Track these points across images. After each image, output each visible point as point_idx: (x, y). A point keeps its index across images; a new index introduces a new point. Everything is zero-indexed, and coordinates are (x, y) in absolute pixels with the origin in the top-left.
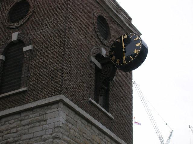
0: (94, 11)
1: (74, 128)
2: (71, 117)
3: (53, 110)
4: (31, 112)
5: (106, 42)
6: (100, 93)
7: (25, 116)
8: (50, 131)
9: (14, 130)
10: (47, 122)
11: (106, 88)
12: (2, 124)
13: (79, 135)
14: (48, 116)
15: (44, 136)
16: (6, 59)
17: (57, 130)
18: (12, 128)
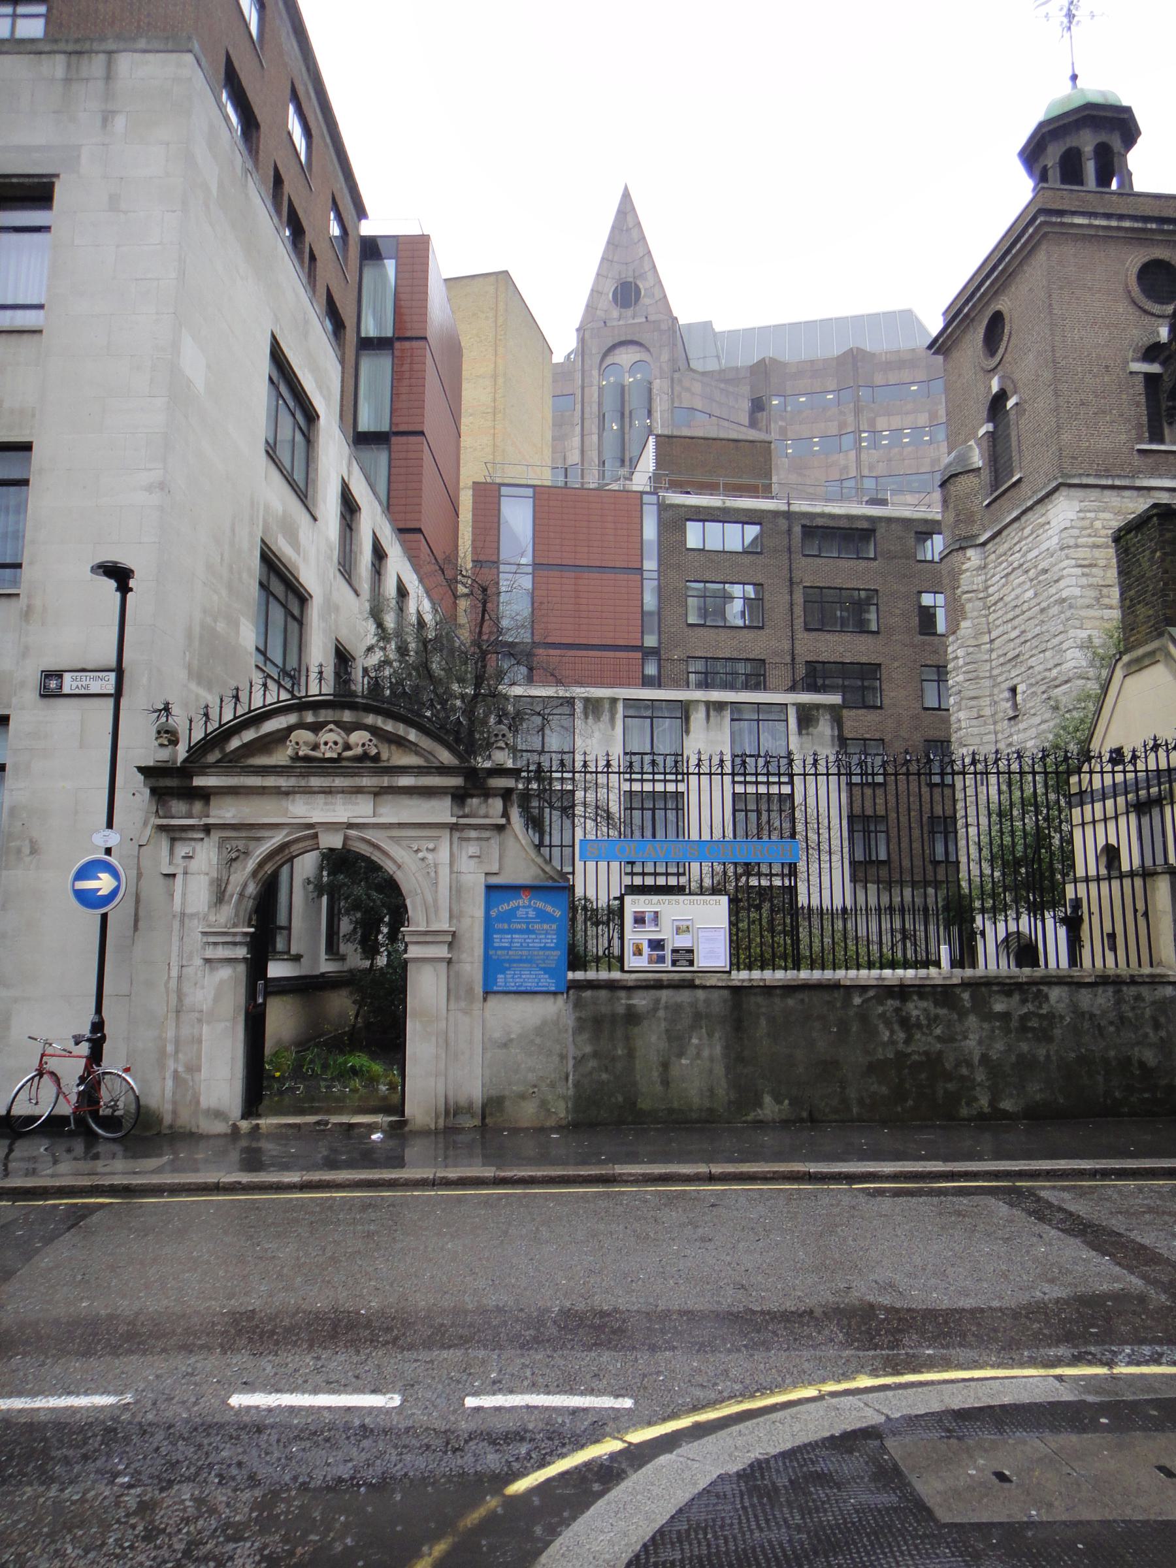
8: (1055, 540)
9: (1017, 548)
14: (1050, 515)
16: (995, 427)
17: (1064, 535)
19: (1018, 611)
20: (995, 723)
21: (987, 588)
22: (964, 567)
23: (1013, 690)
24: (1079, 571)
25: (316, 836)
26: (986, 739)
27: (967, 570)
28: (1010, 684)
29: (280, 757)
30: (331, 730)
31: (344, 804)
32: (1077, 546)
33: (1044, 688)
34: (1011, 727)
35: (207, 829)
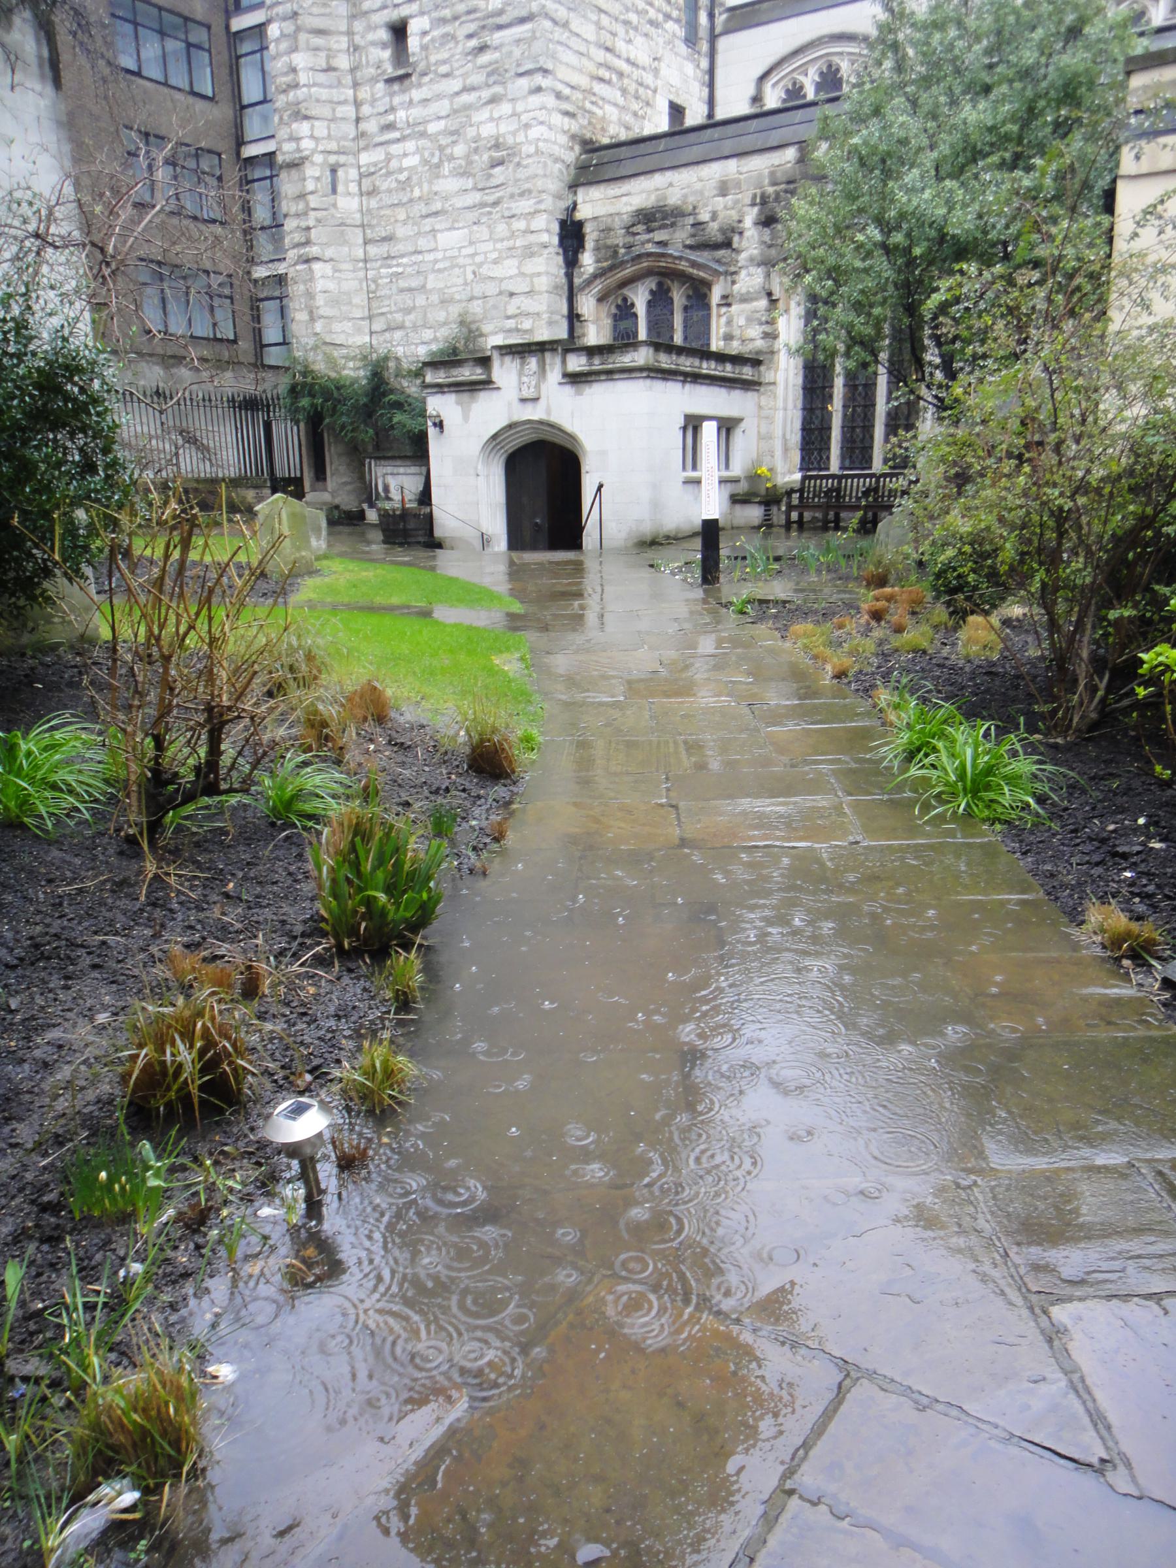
20: (356, 85)
23: (399, 31)
26: (342, 111)
28: (395, 15)
33: (471, 27)
34: (392, 95)
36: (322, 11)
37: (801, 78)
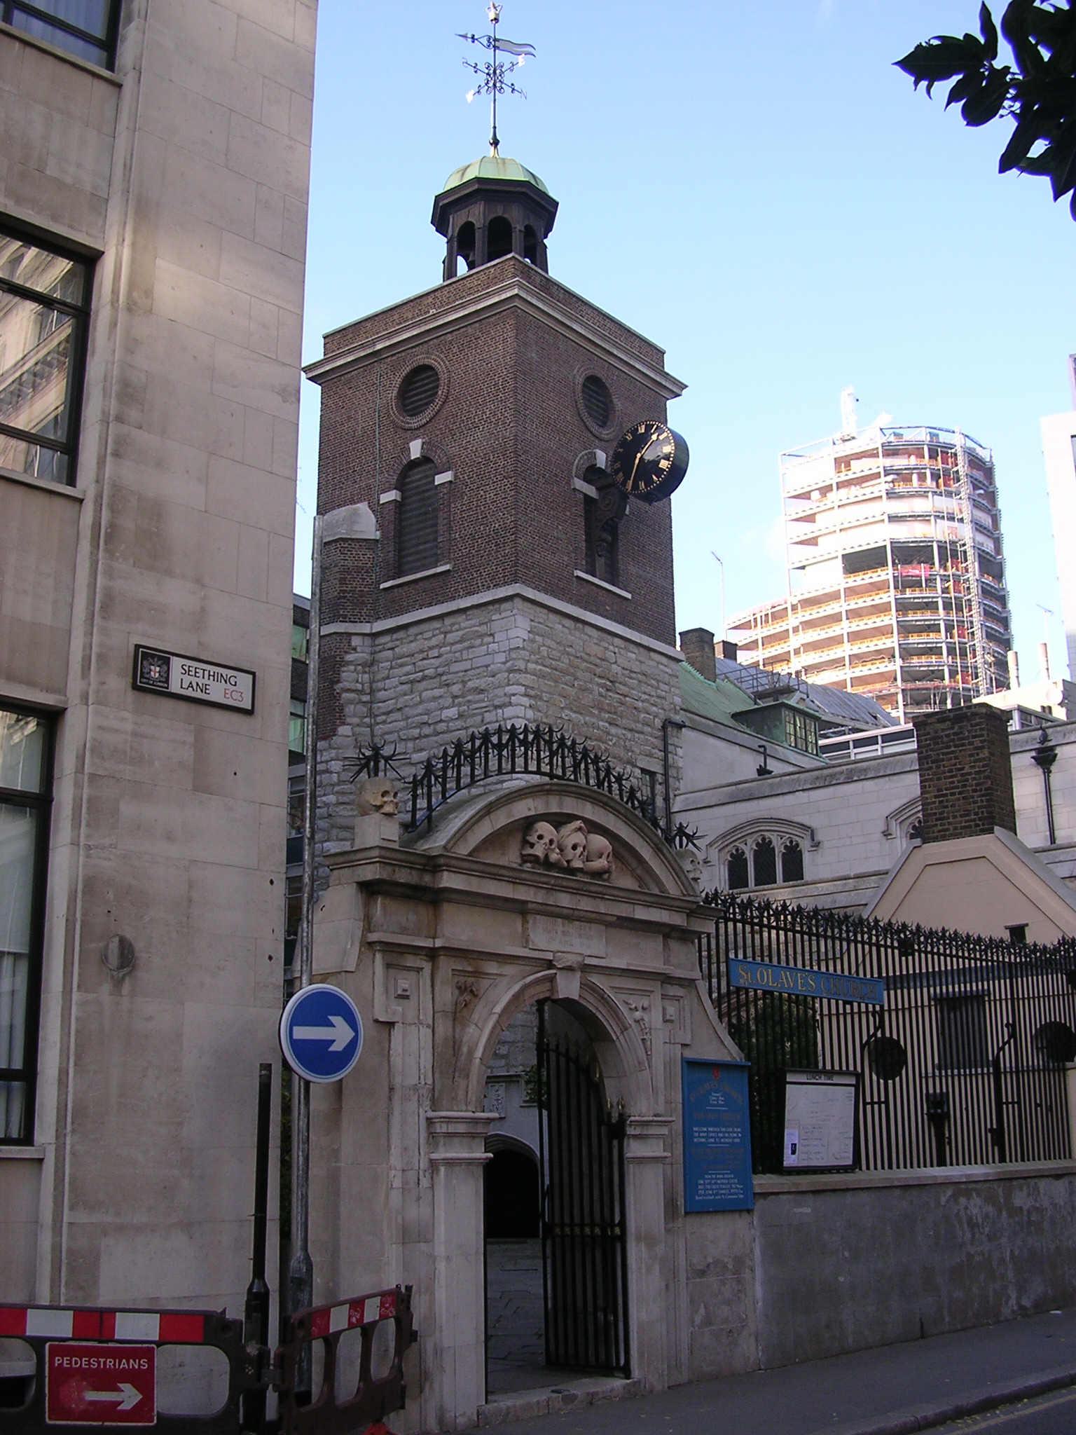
0: (575, 372)
1: (549, 642)
2: (539, 623)
3: (503, 615)
4: (464, 617)
5: (605, 433)
6: (597, 552)
7: (452, 625)
8: (501, 658)
9: (435, 653)
10: (494, 638)
11: (610, 538)
12: (411, 638)
13: (559, 655)
14: (496, 626)
15: (492, 666)
16: (403, 498)
18: (431, 648)
19: (427, 730)
21: (372, 692)
22: (349, 657)
24: (526, 701)
25: (552, 979)
27: (350, 663)
29: (510, 857)
30: (580, 829)
31: (580, 936)
32: (526, 672)
35: (432, 954)
36: (350, 813)
37: (742, 846)
